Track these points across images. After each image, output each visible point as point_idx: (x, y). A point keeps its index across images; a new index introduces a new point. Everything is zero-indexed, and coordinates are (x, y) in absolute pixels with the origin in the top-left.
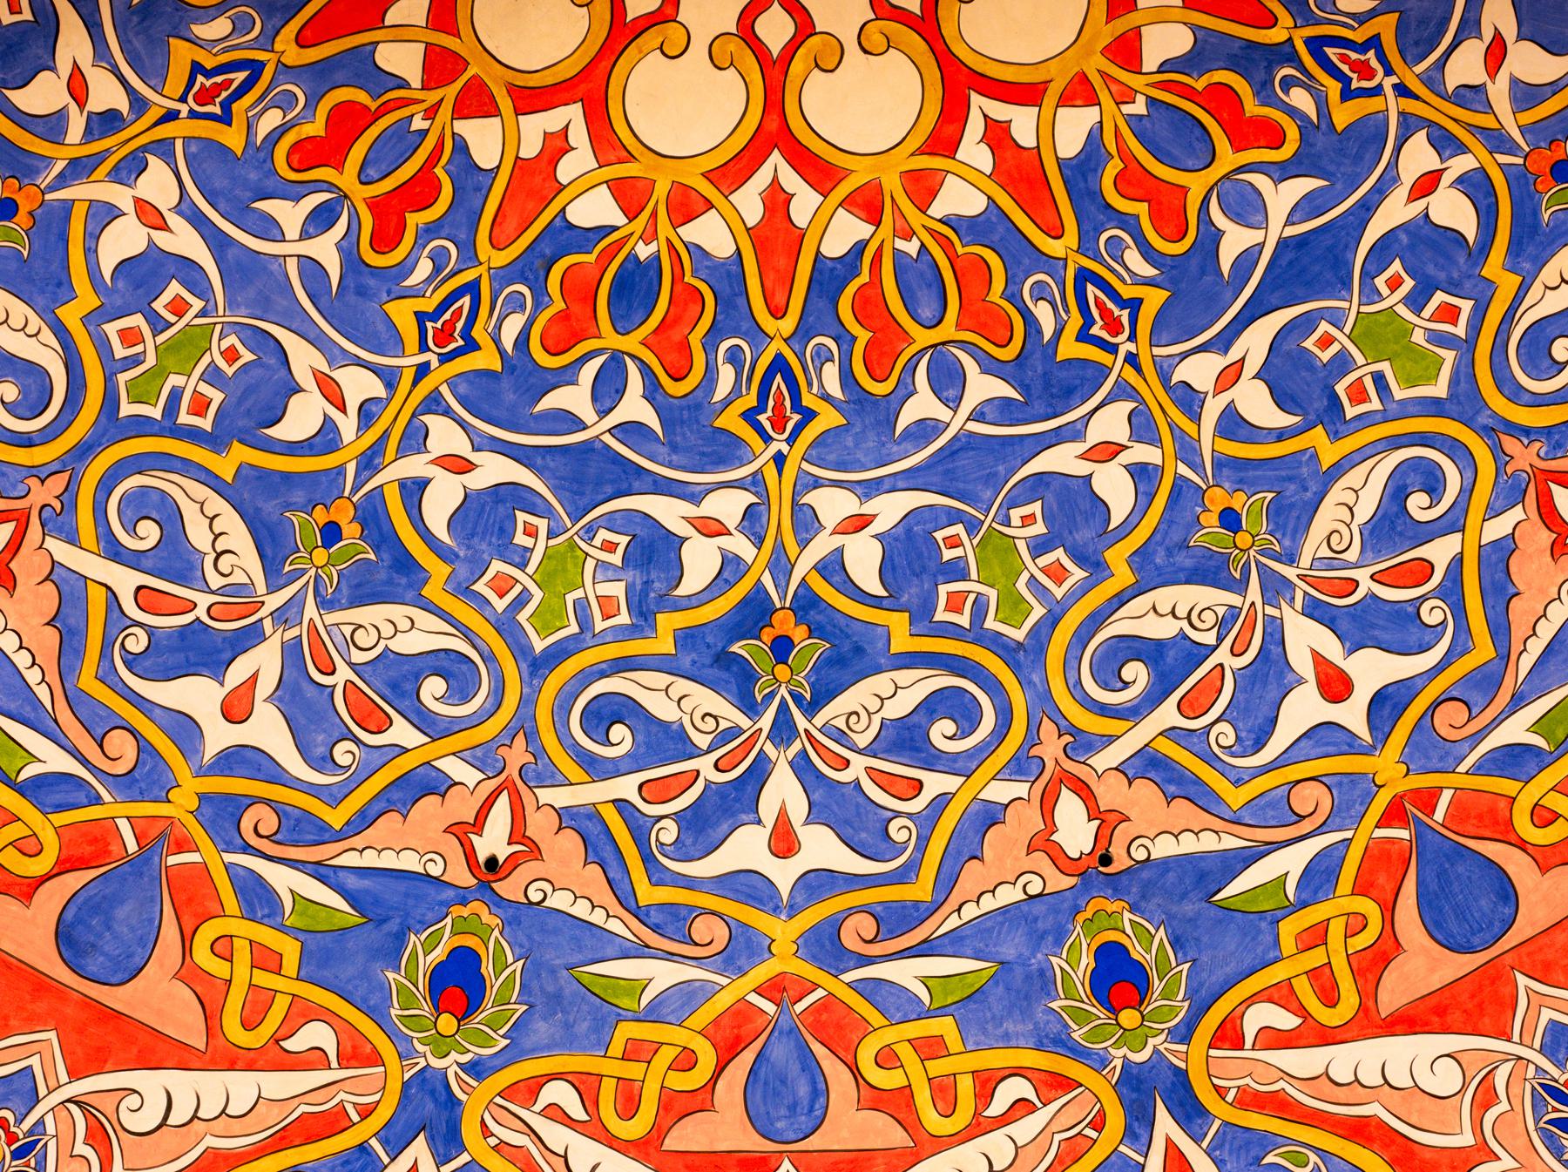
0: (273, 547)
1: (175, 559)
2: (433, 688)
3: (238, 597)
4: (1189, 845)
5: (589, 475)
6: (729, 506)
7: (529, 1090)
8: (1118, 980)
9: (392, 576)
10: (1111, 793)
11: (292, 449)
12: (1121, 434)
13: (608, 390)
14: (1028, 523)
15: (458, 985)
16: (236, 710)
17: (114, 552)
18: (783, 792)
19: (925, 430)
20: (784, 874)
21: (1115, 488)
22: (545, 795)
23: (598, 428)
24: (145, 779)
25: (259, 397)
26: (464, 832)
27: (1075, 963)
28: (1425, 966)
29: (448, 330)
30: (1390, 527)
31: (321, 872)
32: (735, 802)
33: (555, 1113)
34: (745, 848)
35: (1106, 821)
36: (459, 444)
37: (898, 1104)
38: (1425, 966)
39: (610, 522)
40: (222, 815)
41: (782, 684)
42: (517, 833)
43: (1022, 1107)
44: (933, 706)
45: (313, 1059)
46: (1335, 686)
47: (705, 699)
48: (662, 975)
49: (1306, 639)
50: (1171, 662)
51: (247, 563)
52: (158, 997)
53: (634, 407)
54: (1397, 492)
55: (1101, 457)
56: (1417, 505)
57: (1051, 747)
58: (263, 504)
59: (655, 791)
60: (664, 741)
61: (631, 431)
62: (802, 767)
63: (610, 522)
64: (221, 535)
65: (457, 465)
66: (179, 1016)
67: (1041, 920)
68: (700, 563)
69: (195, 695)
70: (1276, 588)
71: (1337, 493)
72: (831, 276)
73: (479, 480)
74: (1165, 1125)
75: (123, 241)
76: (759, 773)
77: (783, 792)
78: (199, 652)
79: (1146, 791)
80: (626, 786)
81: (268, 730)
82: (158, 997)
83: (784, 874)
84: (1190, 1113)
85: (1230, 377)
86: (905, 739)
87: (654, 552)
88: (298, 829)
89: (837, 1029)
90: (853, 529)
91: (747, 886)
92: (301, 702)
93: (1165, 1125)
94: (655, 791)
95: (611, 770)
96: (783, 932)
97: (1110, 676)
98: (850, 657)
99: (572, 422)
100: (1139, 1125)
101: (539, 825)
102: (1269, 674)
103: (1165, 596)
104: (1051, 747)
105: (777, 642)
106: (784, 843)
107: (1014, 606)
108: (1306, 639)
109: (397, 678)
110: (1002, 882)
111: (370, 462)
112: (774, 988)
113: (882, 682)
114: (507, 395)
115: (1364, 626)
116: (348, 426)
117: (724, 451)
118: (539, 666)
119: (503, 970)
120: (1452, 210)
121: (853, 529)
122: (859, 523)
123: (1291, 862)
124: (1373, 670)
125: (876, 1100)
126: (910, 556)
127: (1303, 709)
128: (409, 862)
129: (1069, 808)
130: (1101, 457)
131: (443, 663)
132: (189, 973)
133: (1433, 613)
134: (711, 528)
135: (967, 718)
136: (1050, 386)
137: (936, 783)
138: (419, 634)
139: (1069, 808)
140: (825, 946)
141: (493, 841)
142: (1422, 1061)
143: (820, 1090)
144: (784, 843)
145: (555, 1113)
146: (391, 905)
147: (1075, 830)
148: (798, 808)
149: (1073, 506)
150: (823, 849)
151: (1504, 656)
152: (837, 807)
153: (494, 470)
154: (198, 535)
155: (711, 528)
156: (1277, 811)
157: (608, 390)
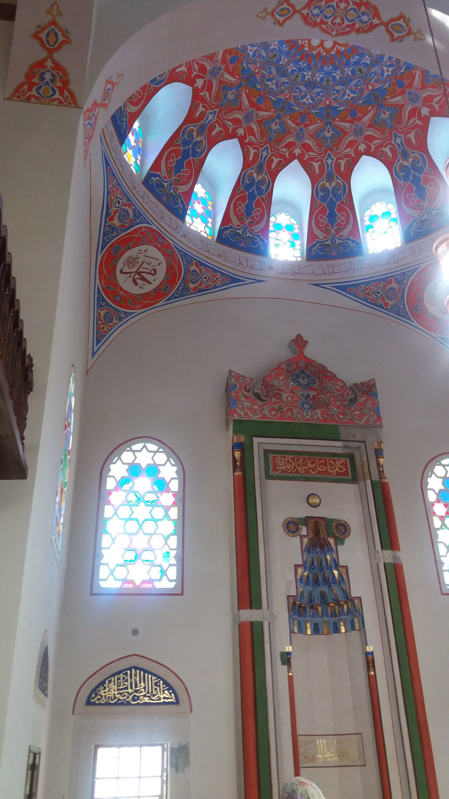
1: (270, 72)
2: (286, 84)
3: (274, 76)
4: (336, 105)
5: (301, 69)
6: (310, 73)
7: (286, 116)
10: (331, 100)
11: (280, 65)
12: (339, 73)
13: (303, 63)
14: (331, 79)
15: (283, 108)
16: (272, 85)
17: (266, 71)
18: (308, 96)
19: (325, 70)
20: (307, 102)
21: (338, 77)
22: (293, 94)
23: (302, 66)
26: (286, 96)
28: (349, 118)
29: (294, 57)
30: (356, 85)
31: (276, 98)
32: (305, 97)
33: (287, 118)
34: (305, 100)
35: (330, 102)
36: (292, 66)
37: (311, 121)
39: (301, 73)
42: (289, 96)
43: (319, 123)
44: (320, 91)
45: (272, 112)
46: (349, 96)
47: (305, 88)
48: (297, 109)
49: (348, 92)
50: (338, 91)
51: (275, 73)
53: (305, 65)
54: (357, 82)
56: (359, 83)
57: (328, 96)
58: (277, 68)
59: (299, 95)
60: (301, 91)
61: (305, 67)
62: (310, 95)
63: (301, 73)
64: (274, 70)
65: (292, 67)
66: (264, 108)
68: (307, 78)
70: (347, 87)
71: (353, 81)
72: (322, 57)
73: (293, 69)
74: (328, 126)
76: (307, 95)
77: (308, 96)
78: (270, 80)
79: (333, 101)
80: (298, 94)
81: (274, 87)
82: (263, 106)
83: (307, 102)
84: (330, 125)
85: (348, 71)
86: (318, 94)
87: (304, 76)
89: (308, 114)
93: (328, 126)
94: (299, 95)
95: (297, 93)
97: (333, 92)
98: (315, 87)
99: (300, 65)
100: (327, 126)
101: (291, 96)
102: (344, 94)
103: (339, 86)
104: (328, 96)
105: (311, 85)
106: (307, 100)
107: (328, 85)
108: (348, 92)
109: (284, 83)
111: (285, 67)
112: (305, 111)
113: (317, 89)
115: (352, 92)
116: (285, 63)
118: (294, 84)
120: (368, 62)
121: (319, 76)
122: (319, 76)
123: (342, 108)
124: (352, 95)
125: (309, 120)
128: (281, 98)
129: (328, 101)
131: (287, 82)
132: (265, 104)
133: (357, 92)
134: (308, 75)
135: (322, 93)
137: (319, 97)
138: (286, 80)
139: (328, 101)
140: (309, 108)
141: (287, 97)
142: (347, 125)
143: (306, 118)
144: (307, 100)
145: (287, 118)
146: (279, 100)
148: (309, 98)
149: (334, 78)
150: (310, 101)
151: (361, 97)
152: (312, 98)
153: (294, 68)
154: (272, 71)
155: (308, 75)
157: (303, 63)
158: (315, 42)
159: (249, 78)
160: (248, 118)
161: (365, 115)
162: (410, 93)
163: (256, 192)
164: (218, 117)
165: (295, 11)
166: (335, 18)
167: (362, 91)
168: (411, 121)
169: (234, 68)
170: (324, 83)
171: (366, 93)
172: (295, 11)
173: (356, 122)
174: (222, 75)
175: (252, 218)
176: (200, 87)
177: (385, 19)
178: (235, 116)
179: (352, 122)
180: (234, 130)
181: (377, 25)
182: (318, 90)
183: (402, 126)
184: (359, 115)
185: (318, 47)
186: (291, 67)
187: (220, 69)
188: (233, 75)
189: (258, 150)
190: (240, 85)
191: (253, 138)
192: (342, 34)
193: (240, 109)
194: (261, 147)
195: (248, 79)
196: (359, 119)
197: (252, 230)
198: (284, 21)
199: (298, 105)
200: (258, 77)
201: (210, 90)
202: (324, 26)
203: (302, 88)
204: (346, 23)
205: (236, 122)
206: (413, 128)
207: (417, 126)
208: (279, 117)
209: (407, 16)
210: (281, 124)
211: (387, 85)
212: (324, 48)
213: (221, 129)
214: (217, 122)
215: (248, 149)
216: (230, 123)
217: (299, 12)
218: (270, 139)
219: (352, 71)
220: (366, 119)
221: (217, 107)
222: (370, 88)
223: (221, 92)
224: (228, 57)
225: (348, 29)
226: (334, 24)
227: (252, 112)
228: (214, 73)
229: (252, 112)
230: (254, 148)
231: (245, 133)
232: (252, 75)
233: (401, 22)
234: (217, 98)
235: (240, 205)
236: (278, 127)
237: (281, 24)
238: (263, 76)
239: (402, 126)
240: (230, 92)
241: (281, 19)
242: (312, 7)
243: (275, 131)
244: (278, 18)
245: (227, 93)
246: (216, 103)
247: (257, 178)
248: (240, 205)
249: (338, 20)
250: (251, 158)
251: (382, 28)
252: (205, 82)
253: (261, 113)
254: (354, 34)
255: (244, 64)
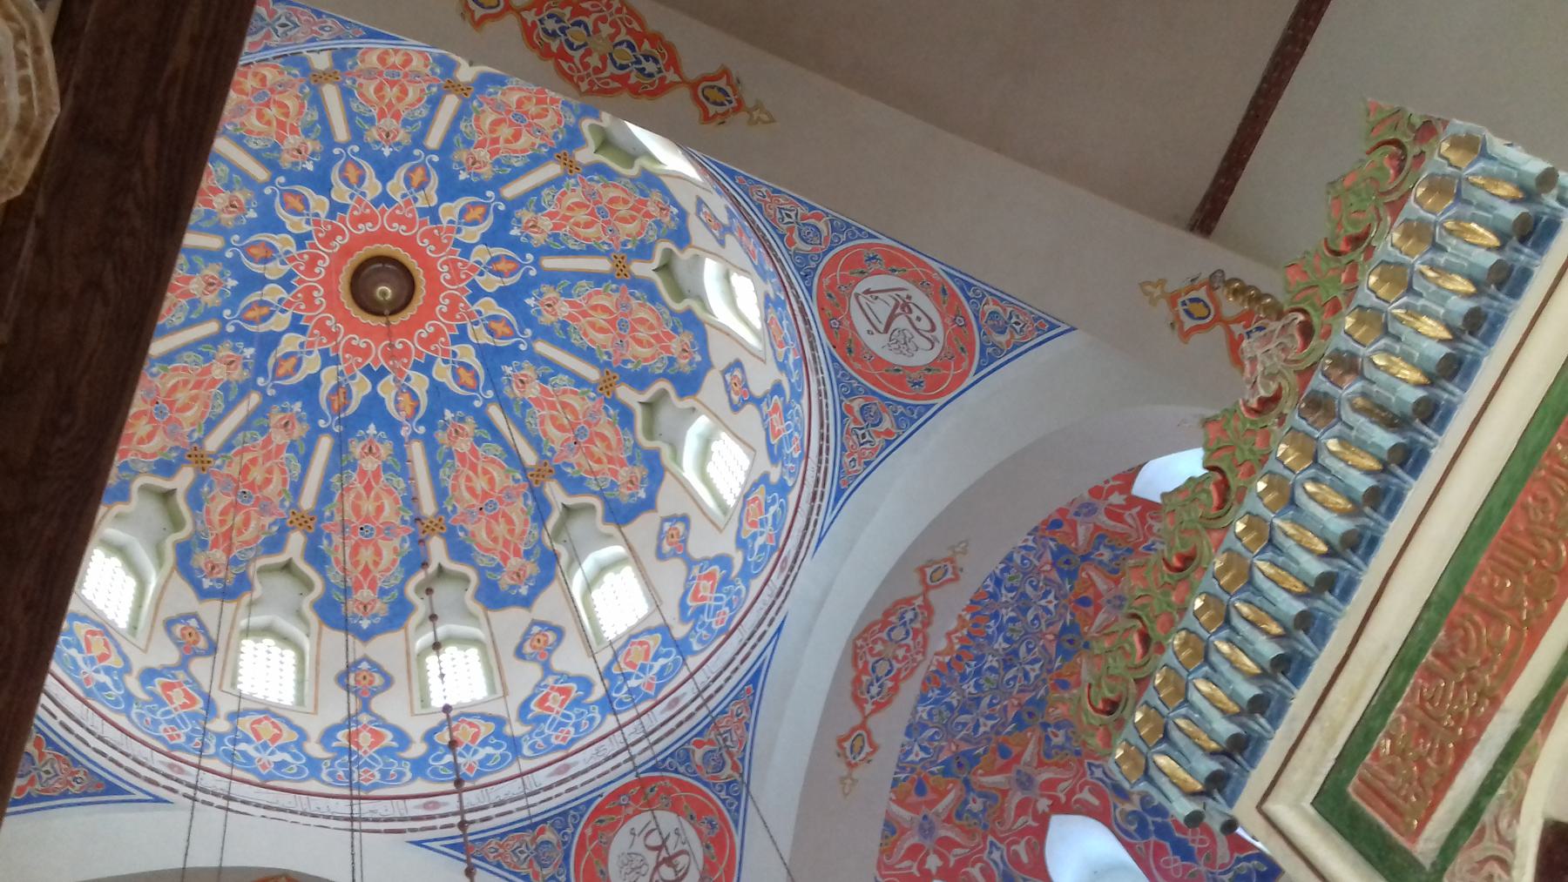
0: (968, 712)
1: (965, 725)
5: (978, 672)
8: (1071, 642)
9: (978, 700)
14: (1010, 625)
15: (1031, 715)
18: (1028, 667)
24: (989, 740)
25: (950, 707)
27: (1067, 645)
29: (953, 681)
34: (1032, 675)
38: (1090, 610)
40: (998, 733)
41: (1015, 661)
48: (1042, 692)
49: (1043, 602)
52: (1015, 750)
55: (1007, 614)
58: (963, 711)
60: (1014, 678)
64: (964, 718)
67: (1059, 646)
68: (995, 664)
69: (982, 730)
72: (969, 634)
75: (925, 716)
77: (1028, 667)
78: (977, 726)
86: (1029, 651)
87: (991, 669)
88: (1004, 725)
90: (1000, 644)
91: (1037, 677)
92: (989, 717)
96: (1045, 675)
98: (1015, 653)
105: (1009, 660)
108: (1043, 602)
109: (991, 705)
110: (1052, 649)
114: (964, 678)
117: (983, 656)
119: (1031, 708)
121: (1000, 644)
123: (1069, 617)
126: (1007, 640)
127: (1051, 607)
130: (1007, 614)
136: (996, 616)
140: (1049, 671)
146: (1017, 718)
147: (1051, 637)
149: (1012, 620)
150: (1037, 666)
156: (1062, 616)
158: (942, 645)
159: (963, 763)
160: (1025, 782)
161: (1093, 585)
162: (1077, 514)
163: (1159, 820)
164: (1002, 840)
165: (863, 726)
166: (896, 658)
167: (1048, 581)
168: (1129, 520)
169: (935, 790)
170: (1016, 637)
171: (1055, 575)
172: (863, 726)
173: (1102, 601)
174: (937, 815)
175: (1201, 851)
176: (940, 863)
177: (920, 589)
178: (1013, 806)
179: (1098, 609)
180: (1036, 817)
181: (926, 600)
182: (1023, 650)
183: (1134, 535)
184: (1090, 594)
185: (950, 640)
186: (969, 687)
187: (925, 817)
188: (948, 792)
189: (1086, 783)
190: (966, 782)
191: (1063, 785)
192: (925, 646)
193: (1005, 793)
194: (1084, 775)
195: (960, 765)
196: (1099, 595)
197: (1222, 866)
198: (871, 744)
199: (1036, 688)
200: (965, 747)
201: (948, 843)
202: (903, 674)
203: (1010, 674)
204: (909, 641)
205: (1022, 808)
206: (1143, 522)
207: (1141, 515)
208: (1045, 726)
209: (922, 563)
210: (1058, 726)
211: (1052, 544)
212: (956, 631)
213: (1023, 843)
214: (1009, 846)
215: (1077, 801)
216: (1021, 821)
217: (866, 718)
218: (1078, 753)
219: (1010, 590)
220: (1102, 585)
221: (984, 838)
222: (1047, 567)
223: (964, 822)
224: (914, 798)
225: (920, 638)
226: (905, 658)
227: (1019, 772)
228: (926, 829)
229: (1019, 772)
230: (1081, 790)
231: (1050, 797)
232: (957, 756)
233: (929, 571)
234: (969, 833)
235: (1167, 863)
236: (1061, 733)
237: (875, 748)
238: (965, 739)
239: (1134, 535)
240: (971, 805)
241: (867, 749)
242: (867, 696)
243: (1068, 739)
244: (863, 755)
245: (970, 811)
246: (978, 839)
247: (1134, 806)
248: (1167, 863)
249: (901, 653)
250: (1095, 801)
251: (933, 596)
252: (936, 852)
253: (1026, 757)
254: (930, 630)
255: (934, 769)
